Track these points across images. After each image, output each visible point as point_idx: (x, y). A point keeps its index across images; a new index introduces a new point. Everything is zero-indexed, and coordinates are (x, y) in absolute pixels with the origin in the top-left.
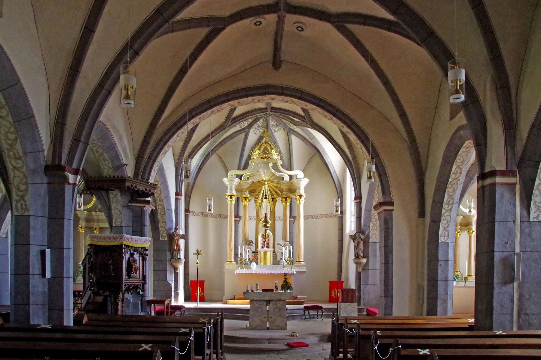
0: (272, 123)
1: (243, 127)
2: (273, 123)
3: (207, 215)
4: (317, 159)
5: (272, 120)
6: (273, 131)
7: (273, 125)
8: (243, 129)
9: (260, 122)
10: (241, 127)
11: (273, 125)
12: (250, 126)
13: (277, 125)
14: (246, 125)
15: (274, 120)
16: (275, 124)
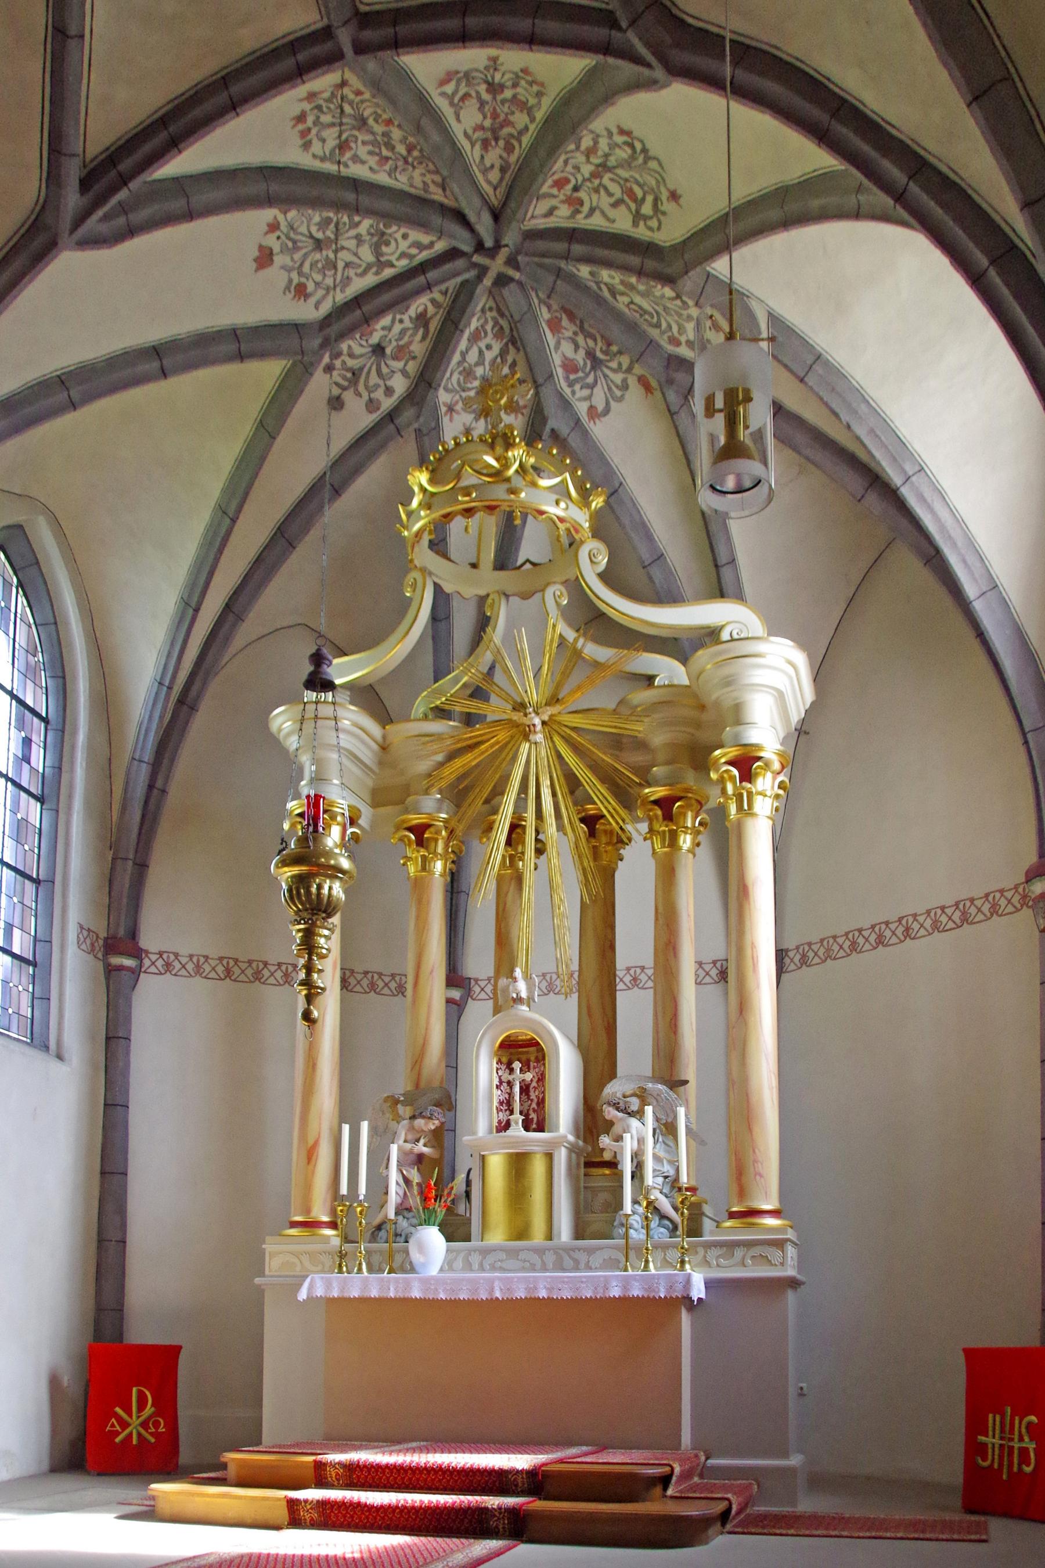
0: (561, 349)
1: (387, 404)
2: (567, 348)
3: (258, 976)
4: (906, 563)
5: (555, 326)
6: (582, 408)
7: (570, 367)
8: (391, 416)
9: (476, 351)
10: (372, 405)
11: (570, 367)
12: (425, 382)
13: (596, 364)
14: (400, 385)
15: (569, 328)
16: (580, 357)
